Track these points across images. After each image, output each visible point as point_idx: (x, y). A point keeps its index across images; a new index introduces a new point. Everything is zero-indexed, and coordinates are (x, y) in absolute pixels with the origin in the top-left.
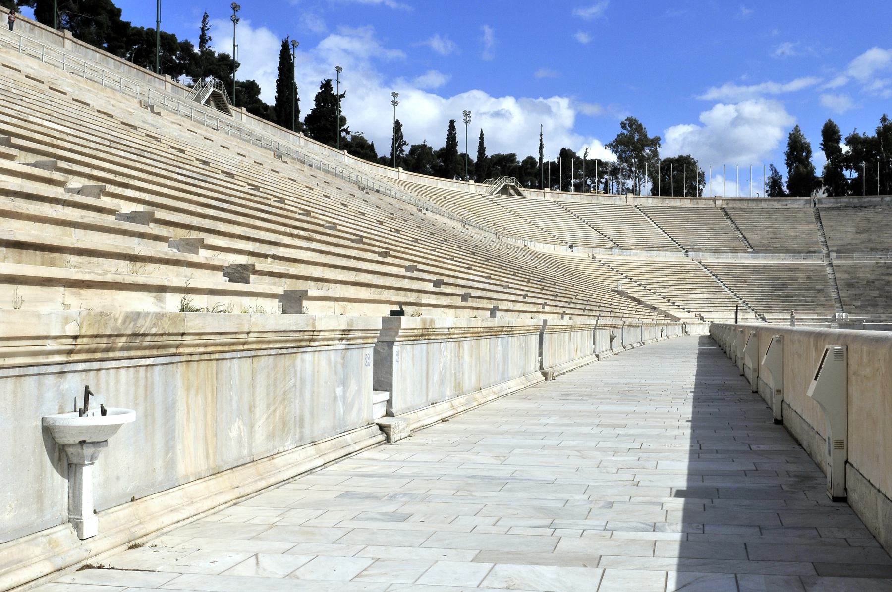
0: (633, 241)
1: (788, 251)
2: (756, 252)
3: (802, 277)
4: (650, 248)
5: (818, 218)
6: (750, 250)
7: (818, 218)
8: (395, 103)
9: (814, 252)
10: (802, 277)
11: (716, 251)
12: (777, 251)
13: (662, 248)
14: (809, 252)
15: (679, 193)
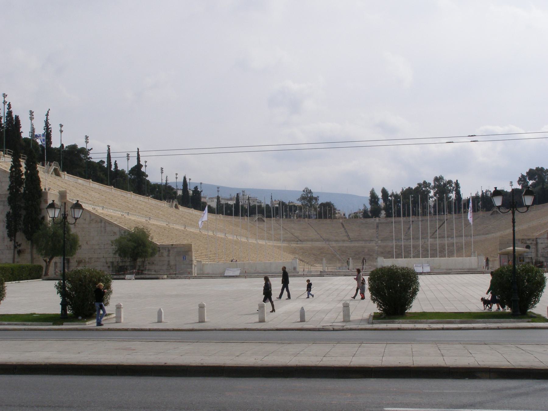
0: (306, 238)
1: (363, 240)
2: (351, 241)
3: (366, 250)
4: (312, 240)
5: (377, 227)
6: (350, 240)
7: (377, 227)
8: (218, 191)
9: (373, 241)
10: (366, 250)
11: (336, 241)
12: (359, 240)
13: (317, 240)
14: (371, 241)
15: (325, 217)
